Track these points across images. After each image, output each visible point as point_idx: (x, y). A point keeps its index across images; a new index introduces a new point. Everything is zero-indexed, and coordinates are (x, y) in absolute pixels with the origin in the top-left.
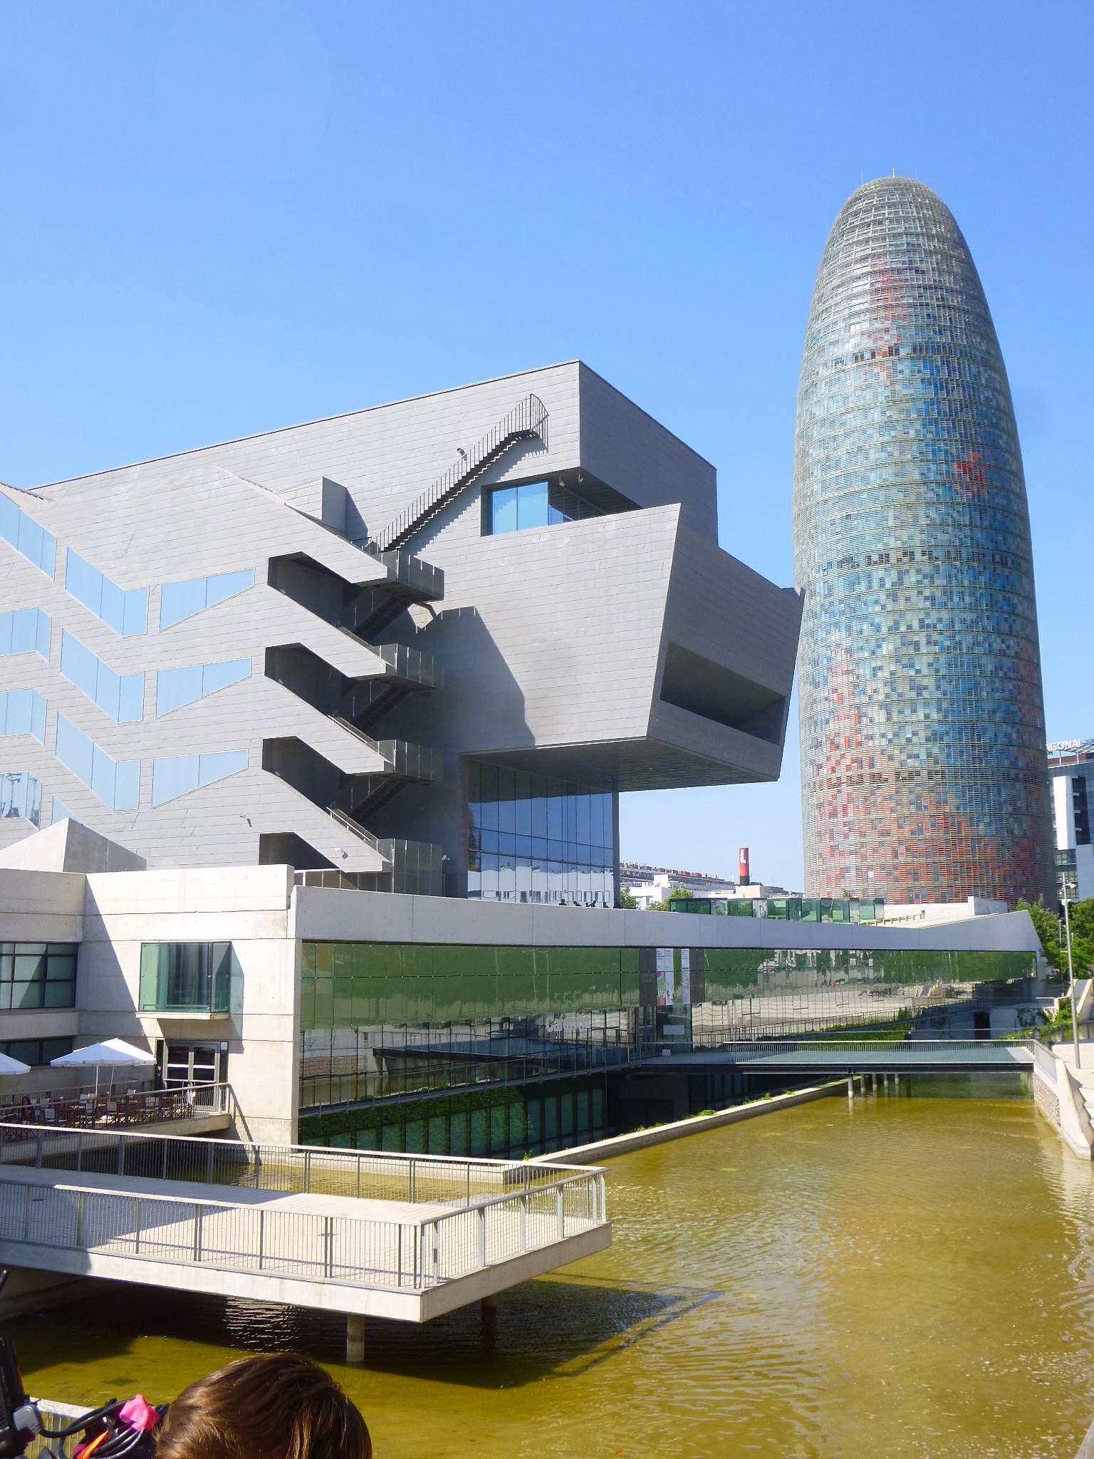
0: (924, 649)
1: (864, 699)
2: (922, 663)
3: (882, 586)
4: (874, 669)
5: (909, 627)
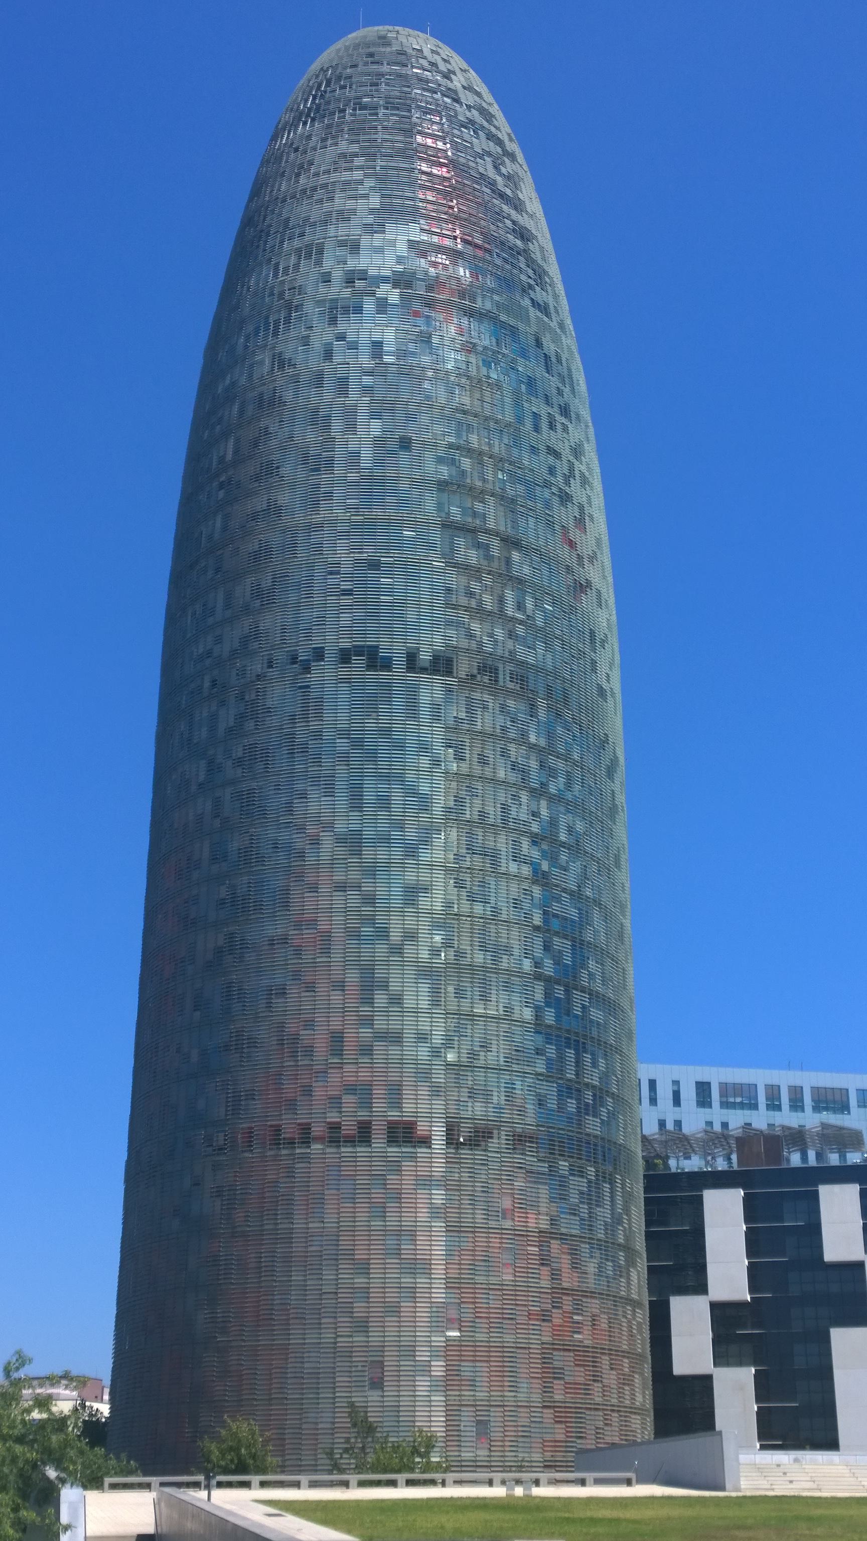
1: (381, 949)
2: (503, 894)
5: (483, 814)
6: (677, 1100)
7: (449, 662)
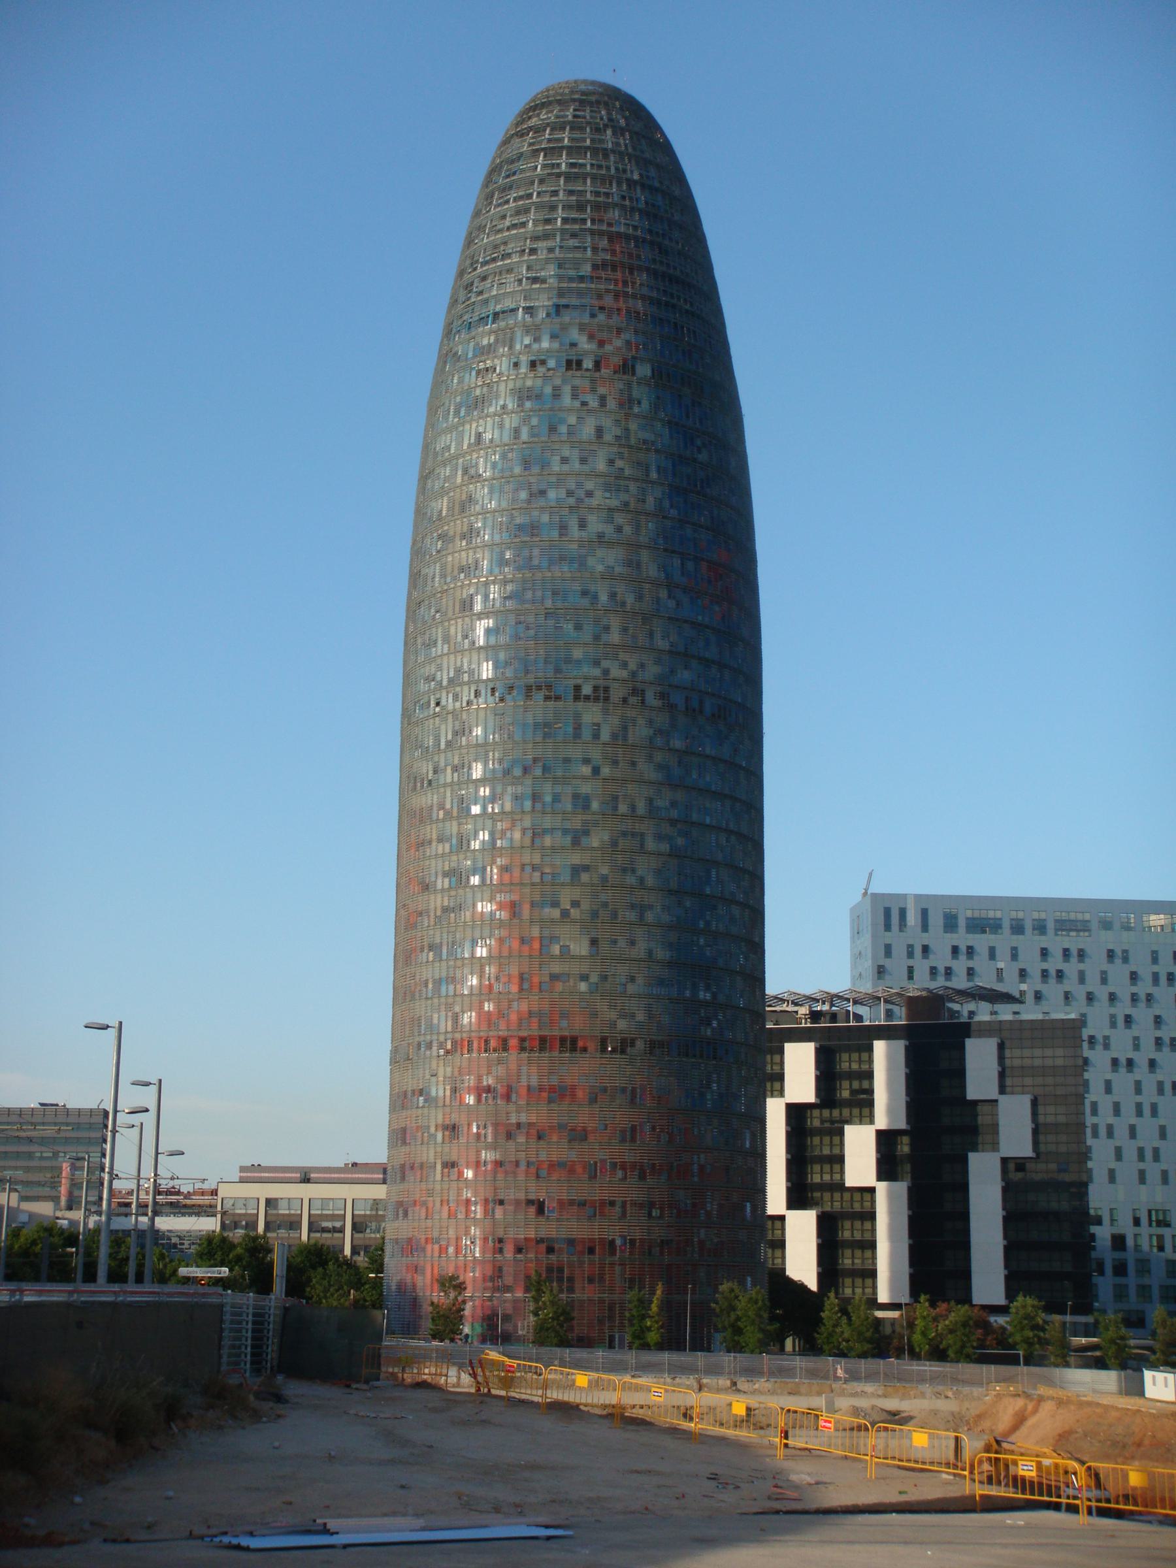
0: (651, 844)
1: (556, 913)
3: (596, 736)
6: (925, 927)
7: (606, 689)
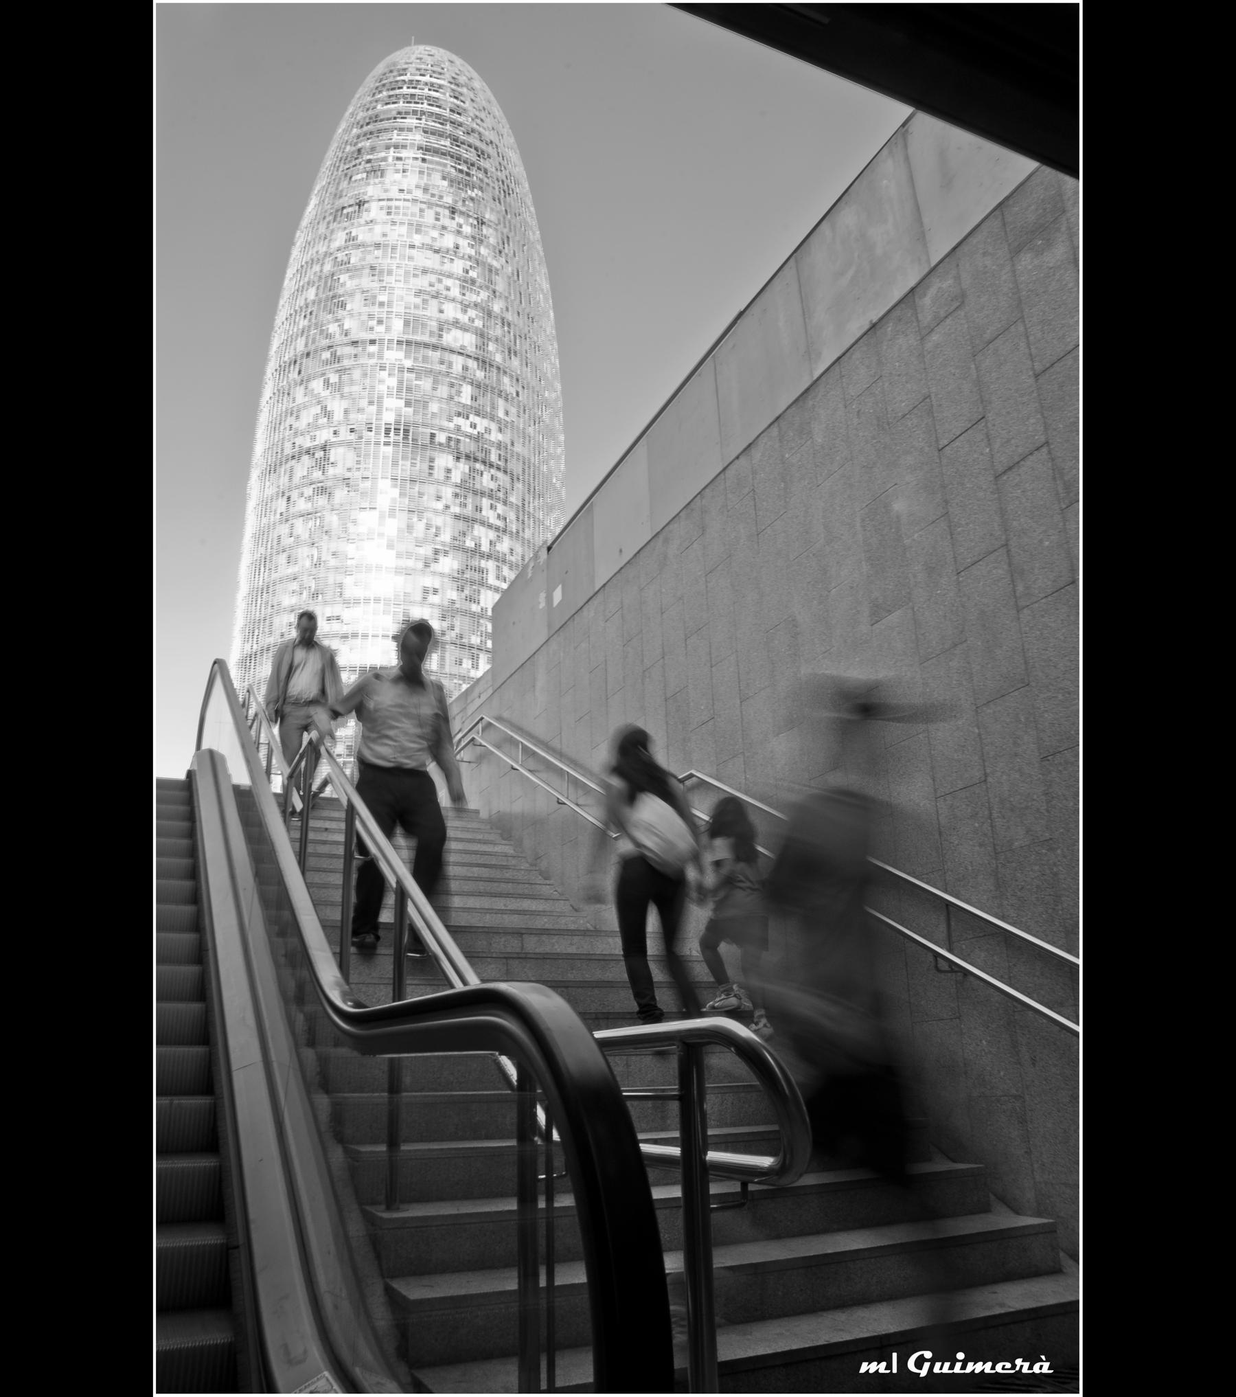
0: (492, 580)
4: (426, 591)
